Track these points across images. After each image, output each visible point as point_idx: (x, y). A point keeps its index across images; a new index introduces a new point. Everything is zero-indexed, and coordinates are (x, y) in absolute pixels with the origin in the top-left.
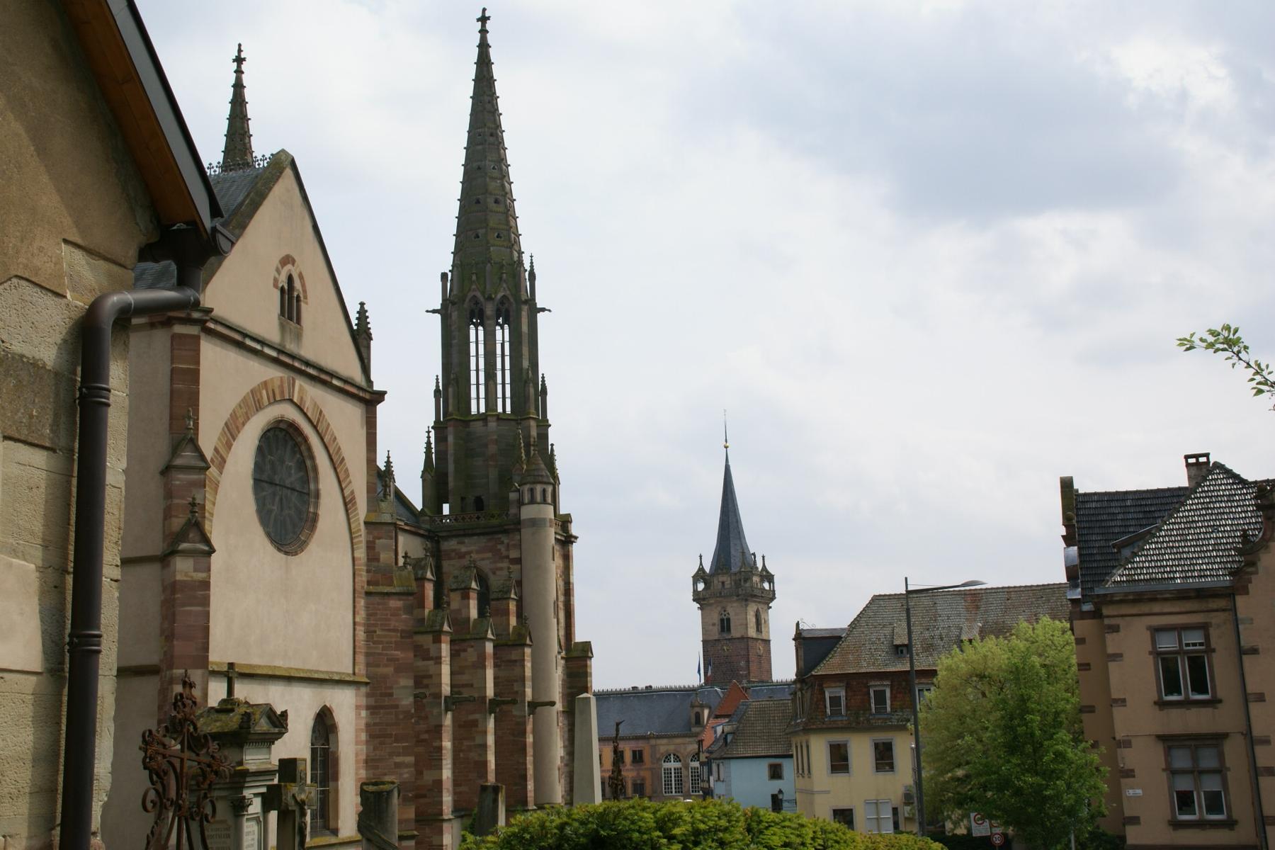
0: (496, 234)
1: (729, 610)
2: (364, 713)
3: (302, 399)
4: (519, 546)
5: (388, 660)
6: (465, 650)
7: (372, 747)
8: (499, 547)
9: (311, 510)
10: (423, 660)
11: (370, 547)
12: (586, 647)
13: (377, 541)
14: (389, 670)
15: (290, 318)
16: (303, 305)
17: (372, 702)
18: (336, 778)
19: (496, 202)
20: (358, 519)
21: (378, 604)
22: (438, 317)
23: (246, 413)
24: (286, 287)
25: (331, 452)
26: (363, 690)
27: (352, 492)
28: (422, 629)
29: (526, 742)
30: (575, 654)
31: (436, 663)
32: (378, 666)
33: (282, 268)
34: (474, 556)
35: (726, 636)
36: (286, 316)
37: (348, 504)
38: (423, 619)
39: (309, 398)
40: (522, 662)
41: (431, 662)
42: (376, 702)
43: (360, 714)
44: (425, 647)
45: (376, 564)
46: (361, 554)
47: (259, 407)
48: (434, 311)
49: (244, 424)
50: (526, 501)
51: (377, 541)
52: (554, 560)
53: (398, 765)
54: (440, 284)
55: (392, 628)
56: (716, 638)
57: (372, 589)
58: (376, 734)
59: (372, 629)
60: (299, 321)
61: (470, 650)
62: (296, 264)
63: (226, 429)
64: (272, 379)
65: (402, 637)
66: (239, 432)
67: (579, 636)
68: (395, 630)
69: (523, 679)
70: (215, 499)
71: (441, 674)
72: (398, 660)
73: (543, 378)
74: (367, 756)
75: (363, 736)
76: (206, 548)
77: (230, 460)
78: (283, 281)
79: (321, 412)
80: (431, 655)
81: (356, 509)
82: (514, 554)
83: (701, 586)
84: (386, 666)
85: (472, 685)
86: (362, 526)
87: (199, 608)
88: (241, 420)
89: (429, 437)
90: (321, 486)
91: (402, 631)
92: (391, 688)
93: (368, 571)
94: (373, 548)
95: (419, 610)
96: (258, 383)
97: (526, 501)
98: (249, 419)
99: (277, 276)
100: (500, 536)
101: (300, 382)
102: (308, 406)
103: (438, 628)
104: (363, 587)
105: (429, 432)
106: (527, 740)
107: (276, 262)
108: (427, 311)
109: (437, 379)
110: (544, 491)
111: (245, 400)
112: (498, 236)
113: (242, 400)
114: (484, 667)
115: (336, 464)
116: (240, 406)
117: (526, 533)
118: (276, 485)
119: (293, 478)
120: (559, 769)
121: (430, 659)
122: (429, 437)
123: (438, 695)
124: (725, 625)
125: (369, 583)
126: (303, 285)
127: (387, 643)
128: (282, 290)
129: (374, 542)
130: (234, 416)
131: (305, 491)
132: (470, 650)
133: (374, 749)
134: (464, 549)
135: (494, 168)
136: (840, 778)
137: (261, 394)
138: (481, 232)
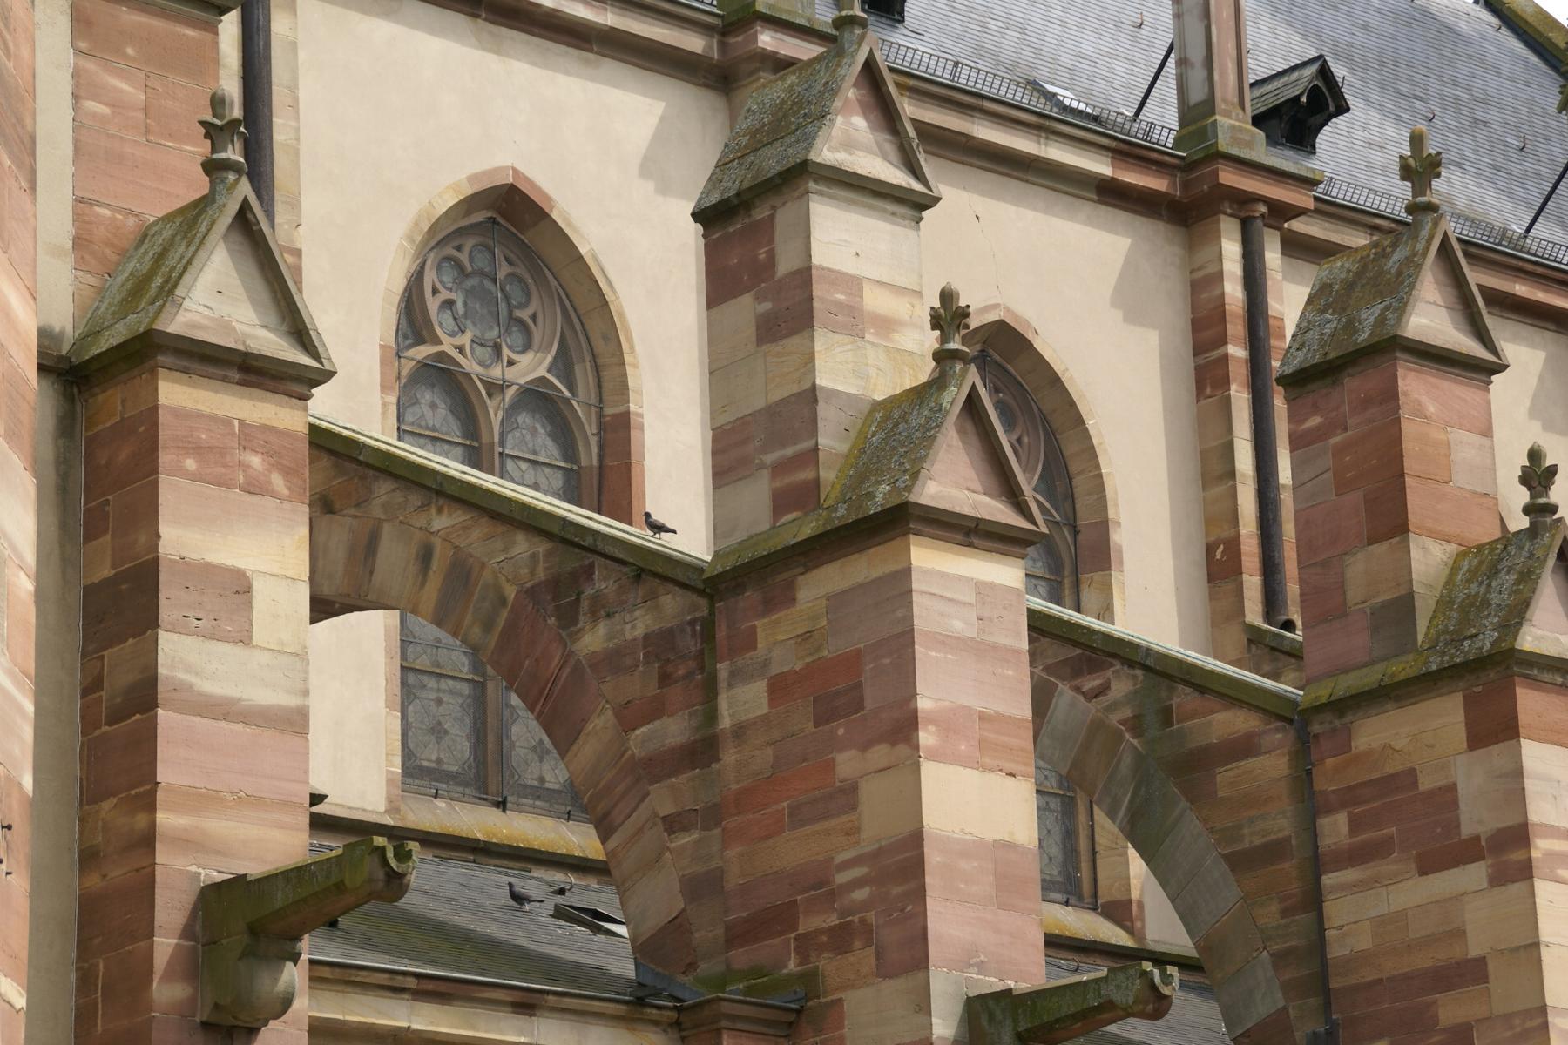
10: (1424, 871)
28: (1403, 668)
31: (1499, 878)
38: (1404, 605)
41: (1474, 875)
44: (1426, 783)
71: (1533, 946)
80: (1467, 830)
95: (1381, 549)
103: (1487, 642)
121: (1469, 852)
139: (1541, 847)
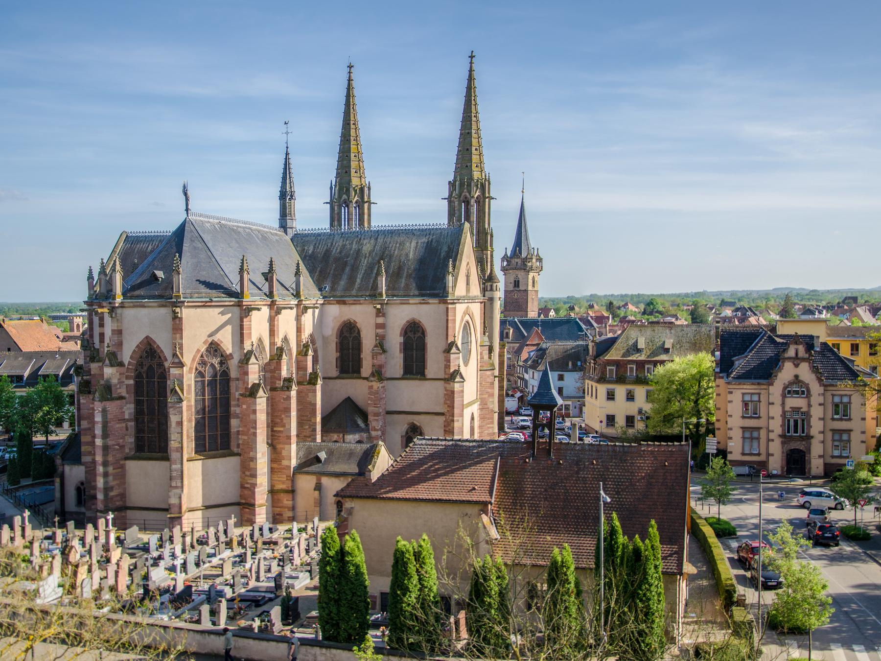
1: (519, 276)
11: (481, 354)
19: (476, 150)
35: (516, 289)
48: (445, 199)
50: (489, 289)
53: (489, 428)
56: (512, 289)
58: (482, 418)
83: (505, 263)
97: (489, 289)
124: (517, 284)
136: (611, 402)
138: (469, 164)
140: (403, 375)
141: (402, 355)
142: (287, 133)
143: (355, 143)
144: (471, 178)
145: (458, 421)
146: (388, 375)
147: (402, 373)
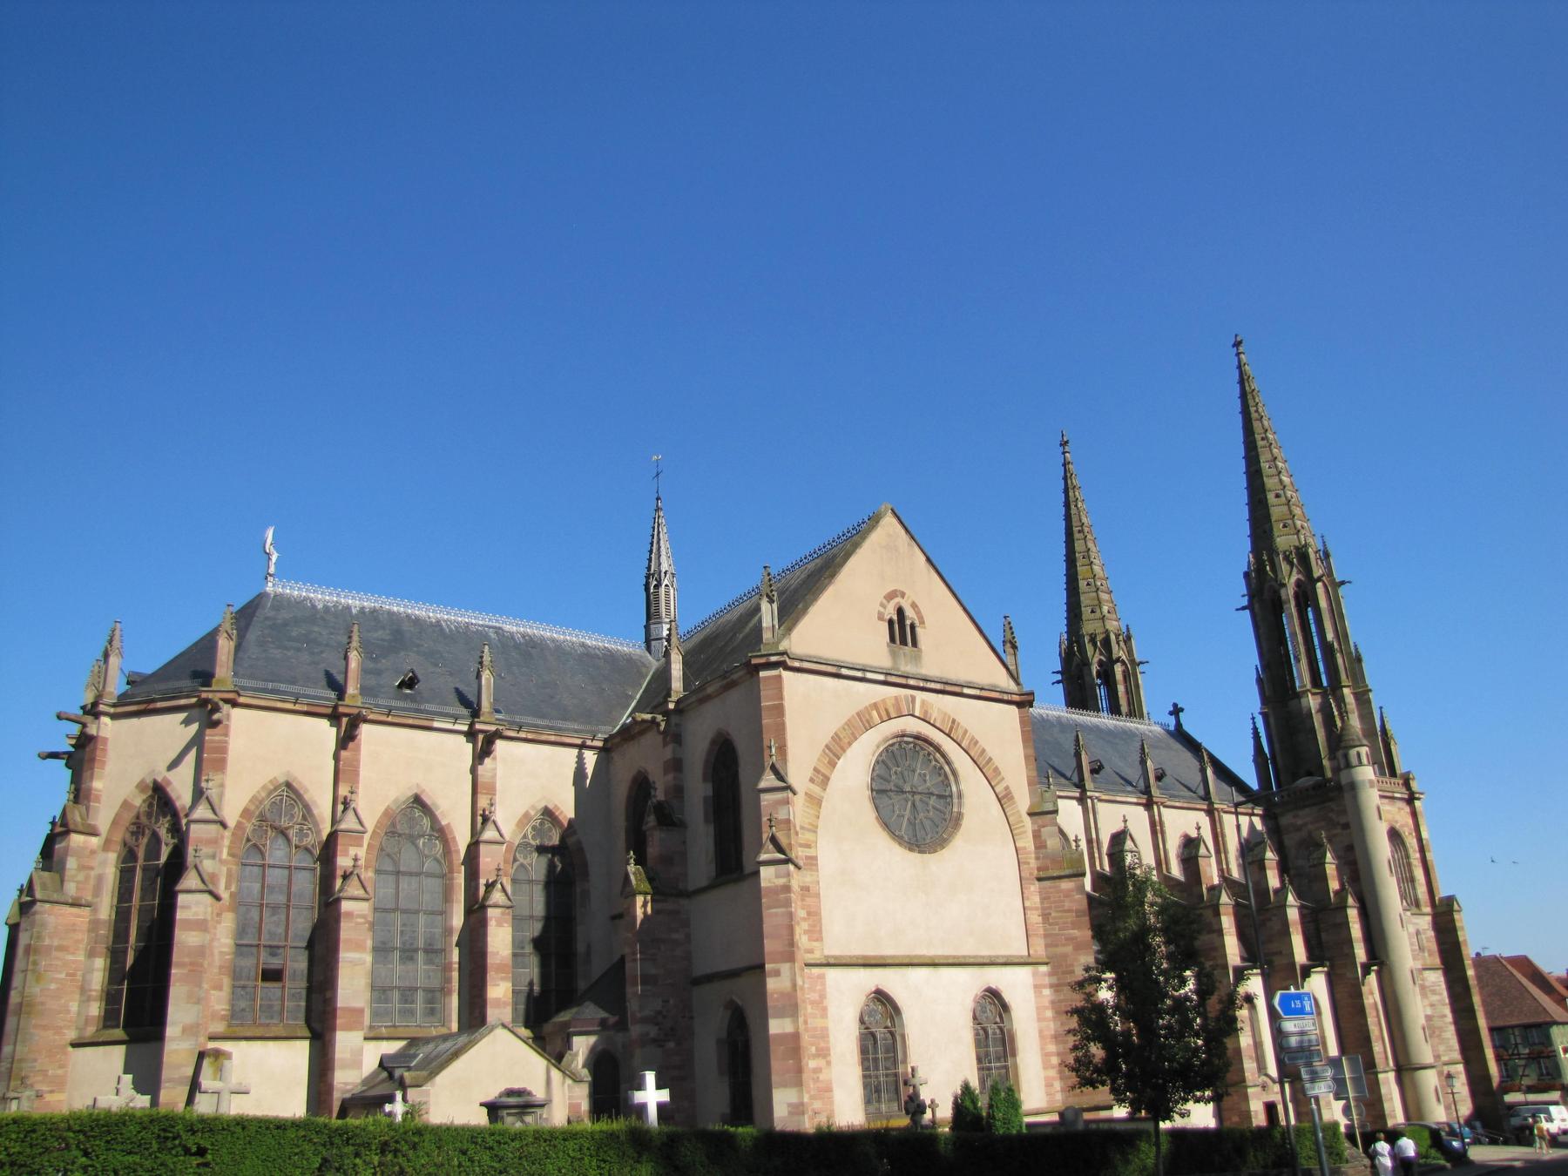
0: (1281, 525)
2: (1047, 992)
3: (926, 712)
4: (1344, 812)
5: (1066, 939)
6: (1270, 920)
7: (1059, 1023)
8: (1330, 815)
9: (955, 809)
11: (1037, 835)
12: (1450, 901)
13: (1042, 829)
14: (1069, 949)
15: (904, 642)
16: (919, 630)
17: (1054, 980)
18: (1014, 1054)
19: (1278, 496)
20: (1018, 811)
21: (1050, 888)
22: (1247, 612)
23: (853, 734)
24: (895, 618)
25: (972, 755)
26: (1044, 969)
27: (1007, 788)
29: (1363, 1004)
30: (1440, 910)
32: (1056, 946)
33: (889, 602)
34: (1310, 827)
36: (898, 642)
37: (1004, 799)
39: (936, 710)
40: (1345, 925)
42: (1058, 979)
43: (1041, 992)
45: (1044, 851)
46: (1028, 843)
47: (869, 726)
48: (1243, 608)
49: (850, 744)
51: (1042, 829)
52: (1380, 818)
54: (1243, 581)
55: (1066, 908)
57: (1042, 874)
59: (1047, 911)
60: (915, 644)
61: (1274, 918)
62: (906, 596)
63: (827, 751)
64: (884, 700)
65: (1077, 916)
66: (844, 751)
67: (1442, 892)
68: (1069, 911)
69: (1349, 941)
70: (819, 812)
72: (1076, 938)
73: (1356, 646)
74: (1056, 1031)
75: (1049, 1014)
76: (783, 857)
77: (835, 776)
78: (891, 613)
79: (954, 721)
81: (1014, 803)
82: (1343, 820)
84: (1064, 945)
85: (1281, 953)
86: (1027, 820)
87: (783, 910)
88: (846, 741)
89: (1254, 723)
90: (962, 787)
91: (1077, 911)
92: (1072, 965)
93: (1037, 858)
94: (1040, 836)
96: (867, 704)
97: (1342, 766)
98: (856, 739)
99: (882, 610)
100: (1330, 804)
101: (920, 696)
102: (934, 716)
104: (1031, 874)
105: (1253, 718)
106: (1365, 1001)
107: (880, 598)
108: (1237, 610)
109: (1257, 669)
110: (1359, 754)
111: (849, 723)
112: (1285, 526)
113: (846, 724)
114: (1288, 935)
115: (982, 763)
116: (844, 728)
117: (1347, 796)
118: (906, 792)
119: (931, 782)
120: (1424, 1029)
122: (1254, 723)
123: (1226, 967)
125: (1039, 869)
126: (918, 613)
127: (1064, 923)
128: (891, 622)
129: (1039, 831)
130: (836, 738)
131: (947, 794)
132: (1274, 918)
133: (1062, 1024)
134: (1300, 822)
135: (1270, 467)
137: (870, 715)
139: (1224, 931)
140: (718, 876)
141: (711, 829)
142: (658, 475)
143: (1086, 561)
144: (1272, 551)
145: (777, 973)
146: (691, 888)
147: (714, 874)
